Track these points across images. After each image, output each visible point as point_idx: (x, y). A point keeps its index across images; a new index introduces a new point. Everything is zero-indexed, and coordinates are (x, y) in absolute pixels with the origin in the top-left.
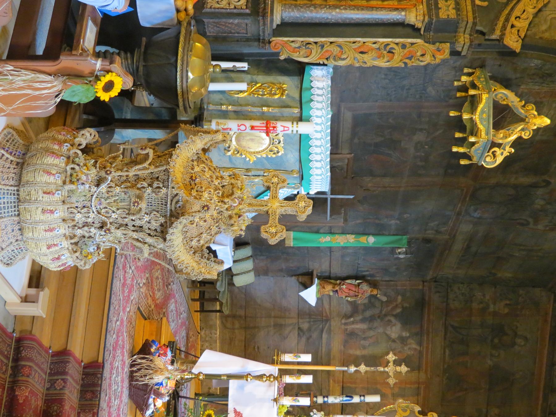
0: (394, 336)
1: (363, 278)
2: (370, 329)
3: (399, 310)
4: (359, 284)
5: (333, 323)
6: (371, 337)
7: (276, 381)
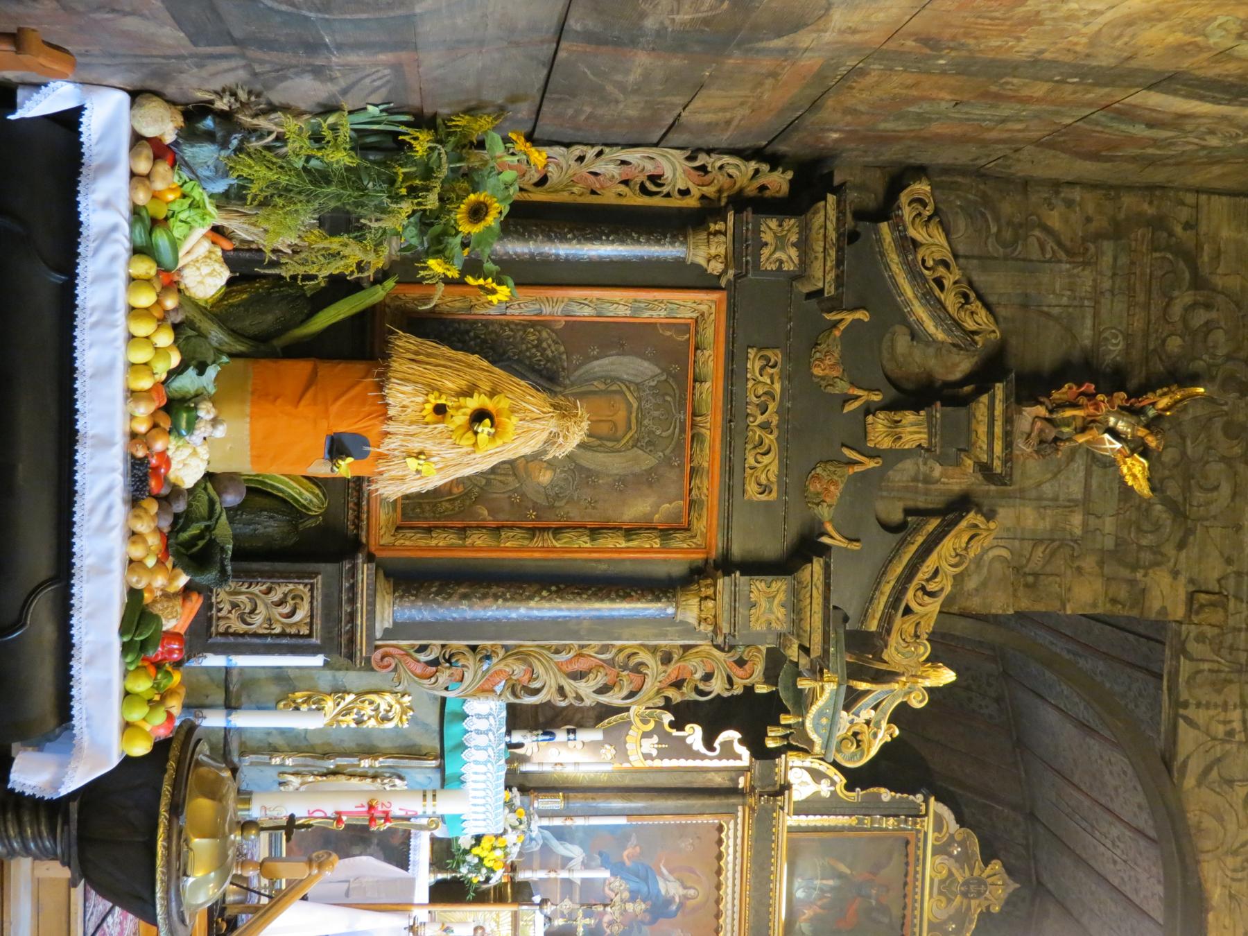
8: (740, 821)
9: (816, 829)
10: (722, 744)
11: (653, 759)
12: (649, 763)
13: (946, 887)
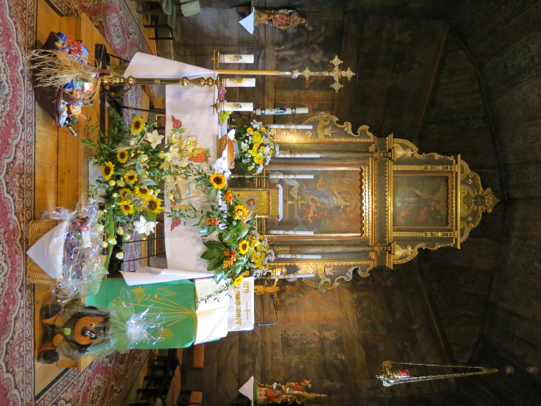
0: (316, 61)
1: (293, 8)
2: (297, 55)
3: (322, 39)
4: (290, 14)
5: (268, 51)
6: (298, 63)
7: (216, 86)
8: (370, 167)
9: (405, 172)
10: (361, 131)
11: (329, 138)
12: (328, 139)
13: (466, 199)
